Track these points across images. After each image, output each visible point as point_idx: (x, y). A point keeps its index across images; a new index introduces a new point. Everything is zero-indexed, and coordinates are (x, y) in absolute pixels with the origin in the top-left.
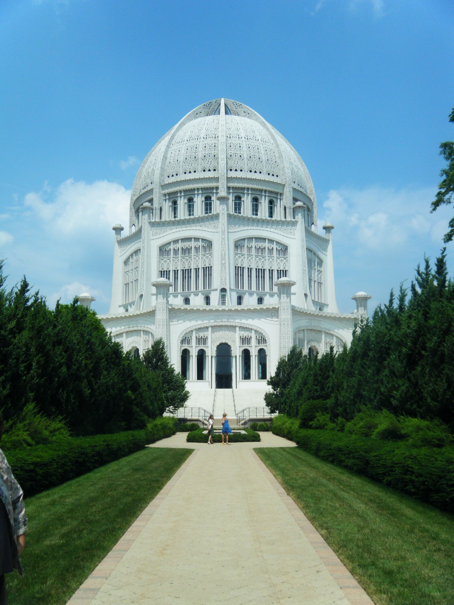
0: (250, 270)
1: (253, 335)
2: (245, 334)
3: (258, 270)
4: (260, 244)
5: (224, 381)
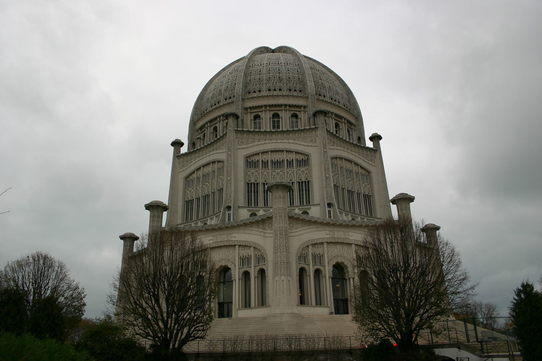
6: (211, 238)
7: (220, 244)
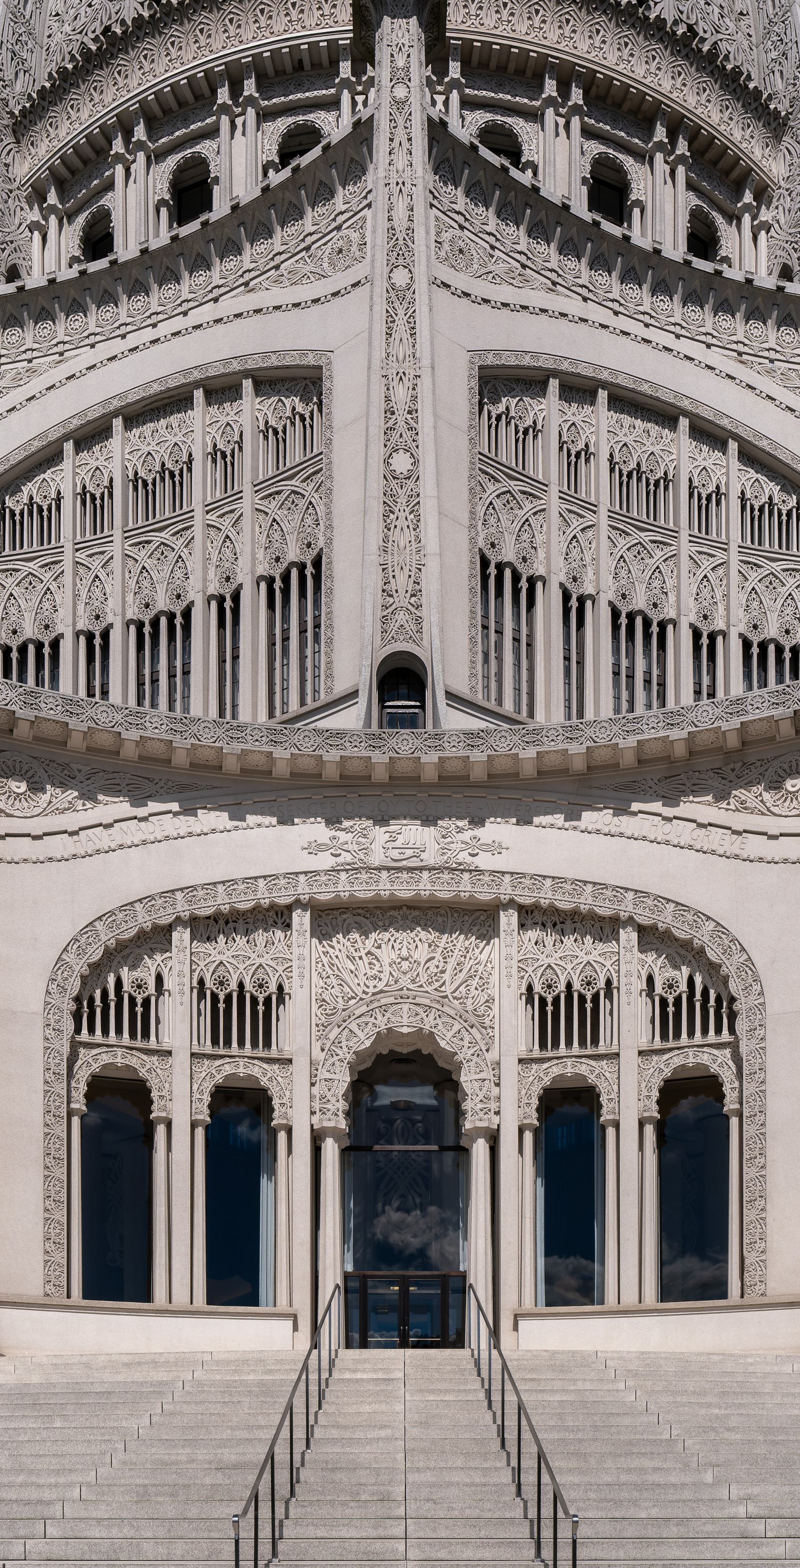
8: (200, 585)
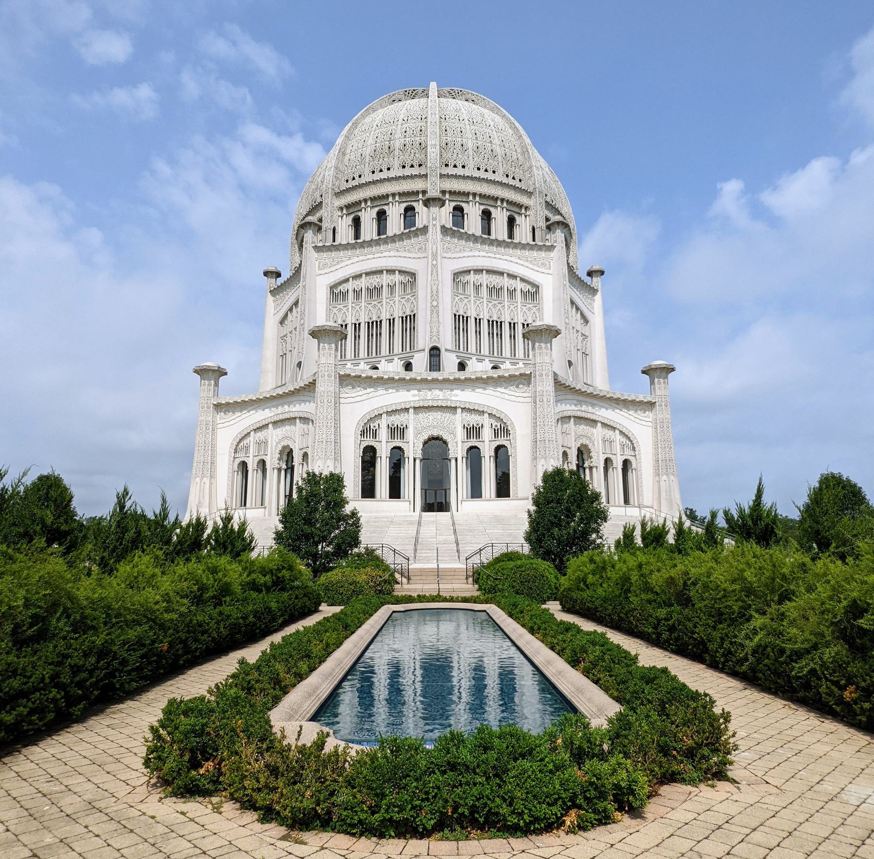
0: (478, 322)
1: (486, 421)
2: (473, 420)
3: (491, 323)
4: (495, 280)
5: (436, 501)
6: (416, 392)
7: (430, 404)
8: (385, 316)
